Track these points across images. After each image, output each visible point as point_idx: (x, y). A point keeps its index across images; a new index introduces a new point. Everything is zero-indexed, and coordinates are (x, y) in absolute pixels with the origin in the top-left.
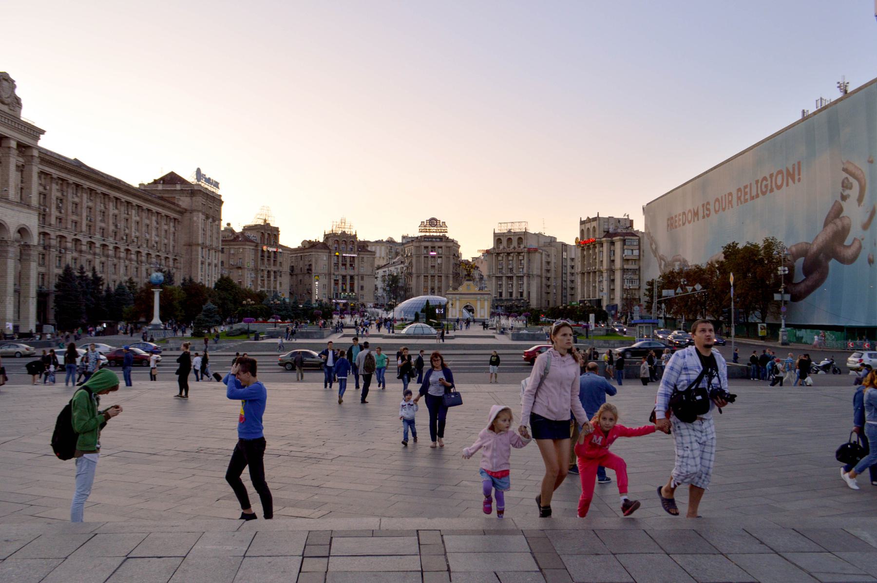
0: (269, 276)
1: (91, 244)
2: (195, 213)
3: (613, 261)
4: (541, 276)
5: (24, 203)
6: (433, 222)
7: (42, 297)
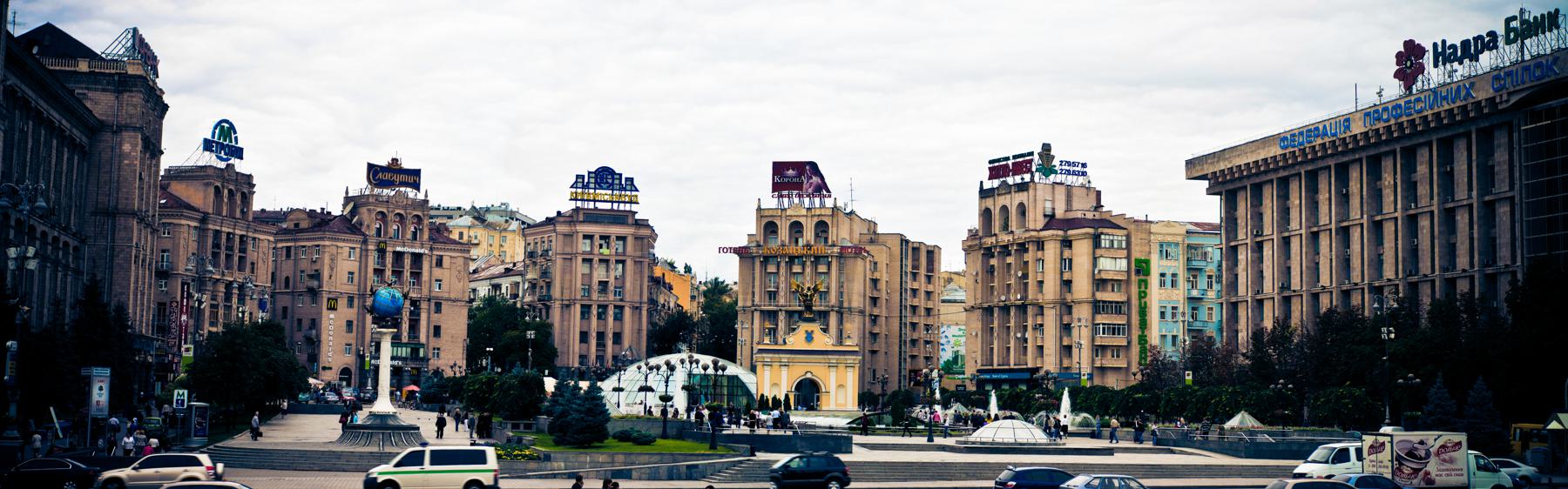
0: (228, 297)
2: (125, 134)
3: (1067, 284)
4: (862, 312)
6: (605, 177)
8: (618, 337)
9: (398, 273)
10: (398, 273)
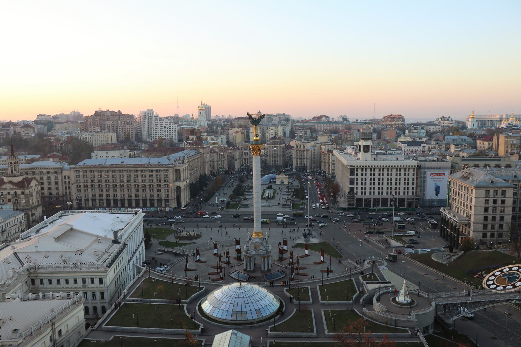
8: (277, 161)
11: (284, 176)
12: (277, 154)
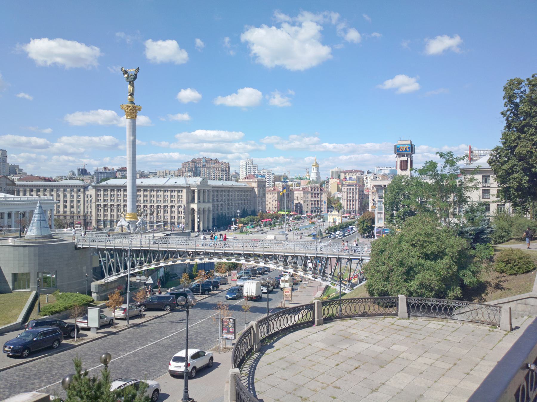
1: (225, 204)
5: (209, 202)
7: (213, 219)
9: (315, 196)
10: (315, 196)
11: (337, 213)
12: (353, 197)
